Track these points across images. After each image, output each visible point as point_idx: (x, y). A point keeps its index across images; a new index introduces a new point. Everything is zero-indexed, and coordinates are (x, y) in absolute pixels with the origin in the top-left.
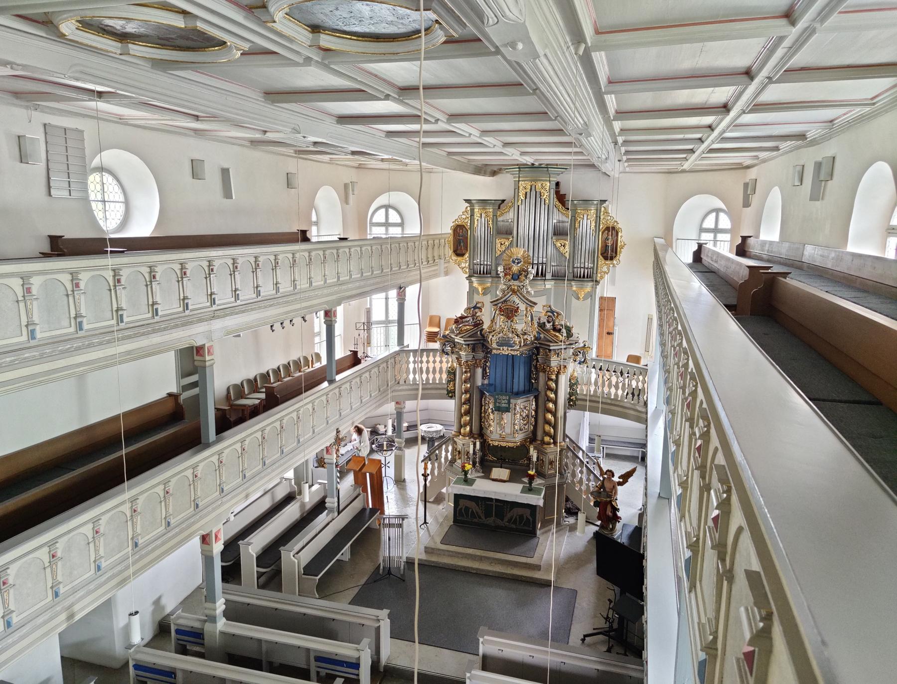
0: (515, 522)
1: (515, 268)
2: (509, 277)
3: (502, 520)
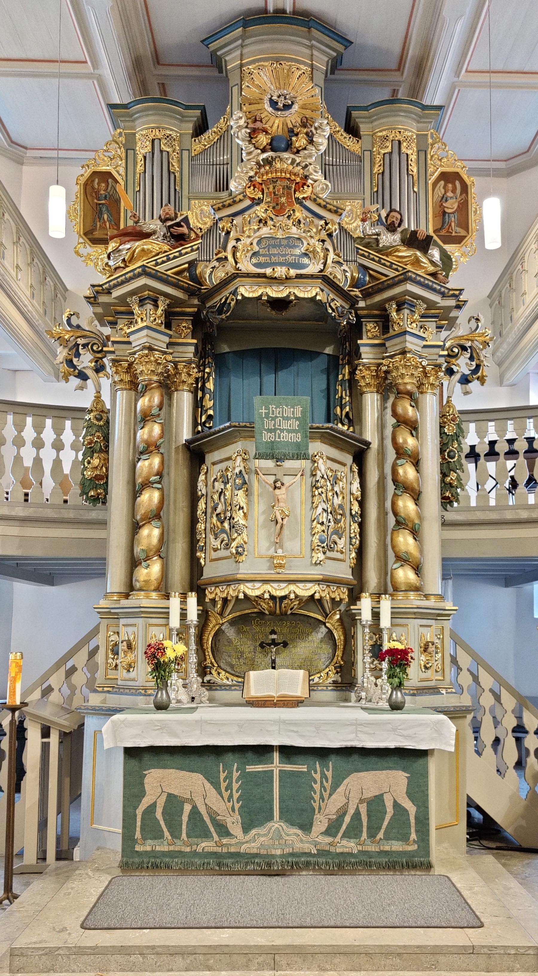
2: (263, 140)
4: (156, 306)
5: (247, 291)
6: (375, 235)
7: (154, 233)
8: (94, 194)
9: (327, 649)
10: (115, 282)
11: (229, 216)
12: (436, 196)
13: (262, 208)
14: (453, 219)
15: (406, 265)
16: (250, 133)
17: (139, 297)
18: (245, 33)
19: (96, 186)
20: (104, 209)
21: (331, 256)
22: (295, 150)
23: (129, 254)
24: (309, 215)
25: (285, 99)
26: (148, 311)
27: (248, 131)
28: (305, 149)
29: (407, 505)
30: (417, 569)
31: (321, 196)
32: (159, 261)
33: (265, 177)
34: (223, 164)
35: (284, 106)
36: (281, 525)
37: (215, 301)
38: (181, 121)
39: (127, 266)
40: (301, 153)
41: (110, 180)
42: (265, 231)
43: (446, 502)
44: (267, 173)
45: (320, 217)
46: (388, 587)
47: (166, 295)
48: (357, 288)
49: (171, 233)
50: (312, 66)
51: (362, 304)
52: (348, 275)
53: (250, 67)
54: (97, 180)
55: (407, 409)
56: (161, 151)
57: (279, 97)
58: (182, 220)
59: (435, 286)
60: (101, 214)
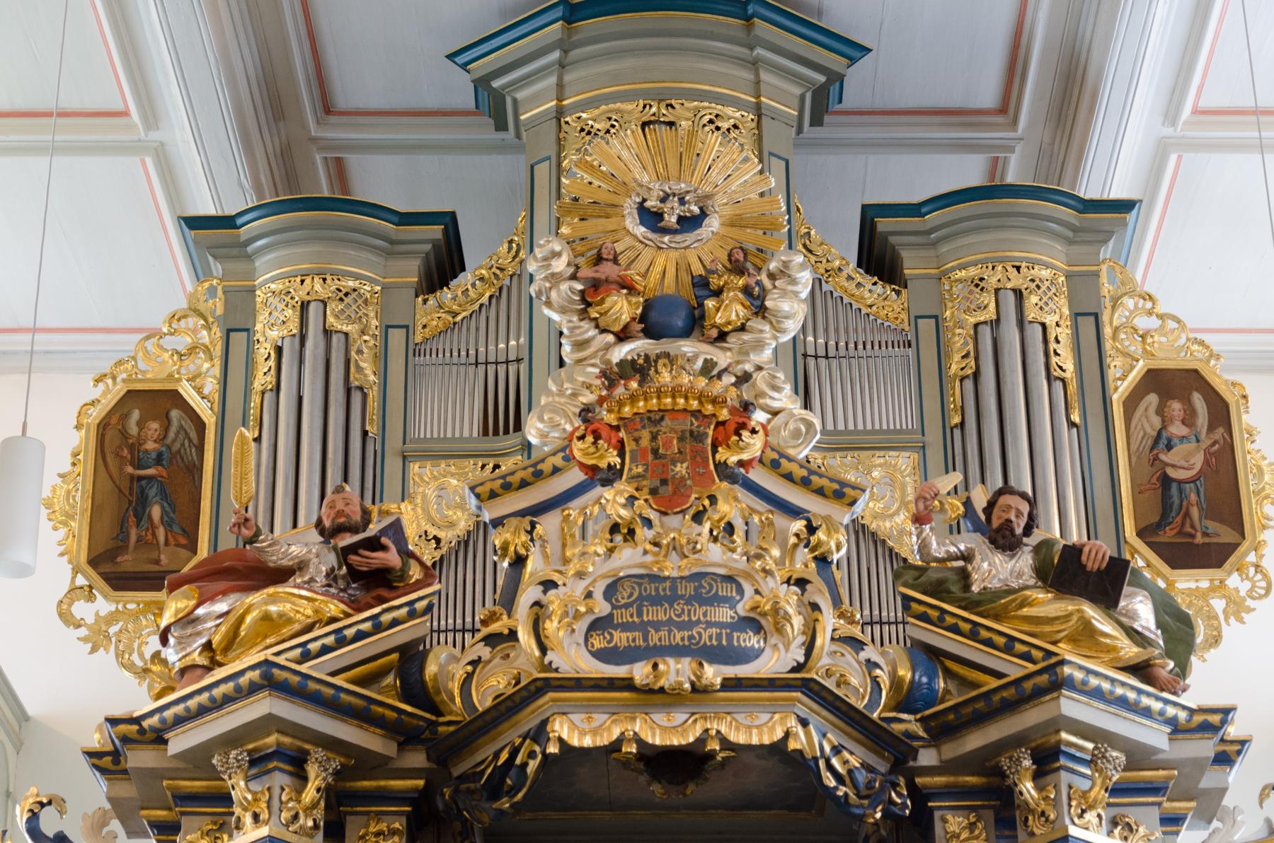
2: (622, 308)
4: (303, 778)
5: (576, 729)
6: (957, 559)
7: (301, 566)
8: (125, 452)
10: (179, 709)
11: (522, 513)
12: (1137, 436)
13: (620, 493)
14: (1193, 497)
15: (1054, 643)
16: (582, 292)
17: (250, 752)
18: (570, 36)
19: (133, 429)
20: (152, 492)
21: (829, 621)
22: (714, 333)
23: (223, 629)
24: (760, 505)
25: (682, 201)
26: (276, 791)
27: (580, 287)
28: (742, 328)
31: (791, 452)
32: (311, 646)
33: (627, 411)
34: (507, 362)
35: (681, 219)
37: (479, 757)
38: (389, 254)
39: (214, 664)
40: (732, 339)
41: (175, 414)
42: (629, 559)
44: (633, 398)
45: (794, 512)
47: (332, 744)
48: (909, 712)
49: (349, 566)
50: (758, 110)
51: (927, 758)
52: (883, 676)
53: (584, 115)
54: (136, 415)
56: (328, 333)
57: (663, 200)
58: (383, 532)
59: (1146, 701)
60: (144, 508)
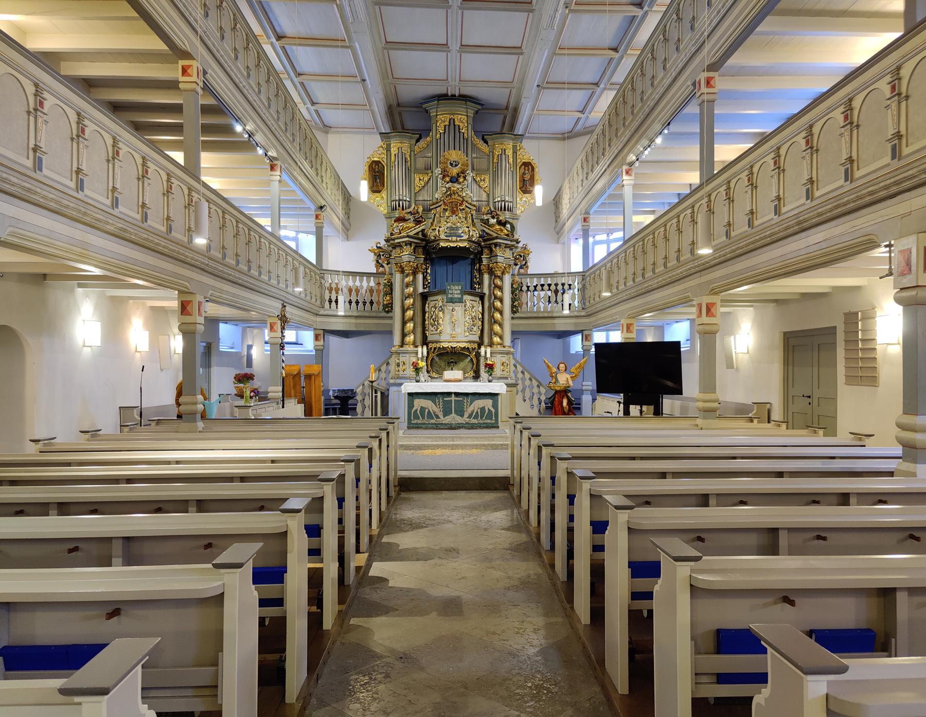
0: (476, 417)
1: (455, 171)
2: (448, 179)
3: (462, 416)
9: (470, 365)
29: (497, 316)
30: (501, 337)
36: (455, 324)
43: (513, 312)
46: (491, 344)
55: (498, 282)
